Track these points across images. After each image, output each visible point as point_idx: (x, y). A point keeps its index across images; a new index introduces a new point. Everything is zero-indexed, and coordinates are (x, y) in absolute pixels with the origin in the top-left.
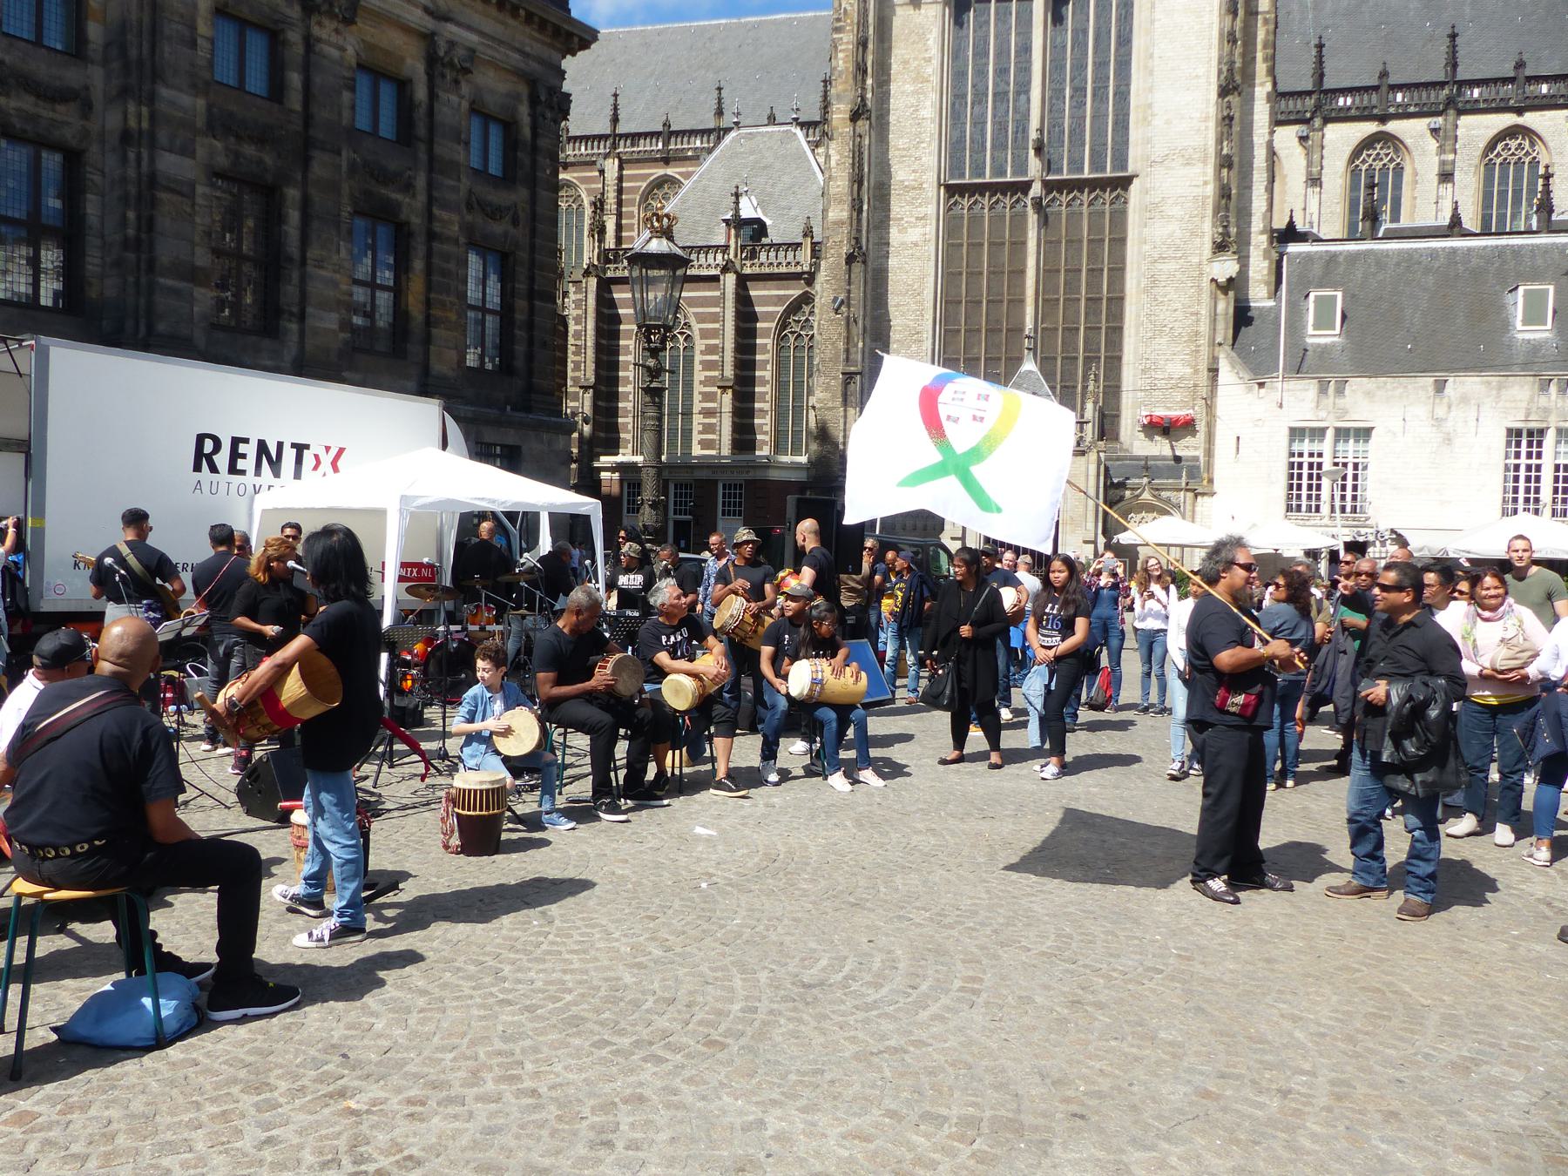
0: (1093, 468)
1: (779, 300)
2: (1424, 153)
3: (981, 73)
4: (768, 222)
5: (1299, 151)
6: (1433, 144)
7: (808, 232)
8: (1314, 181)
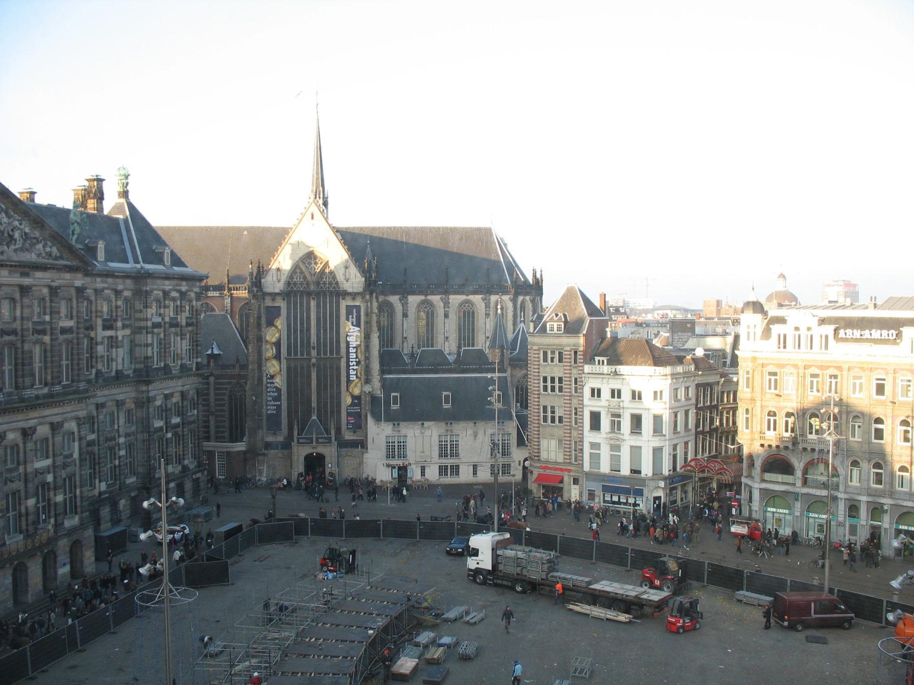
0: (333, 450)
1: (229, 383)
2: (440, 307)
3: (295, 324)
4: (222, 353)
5: (400, 304)
6: (442, 305)
7: (238, 361)
8: (405, 315)
